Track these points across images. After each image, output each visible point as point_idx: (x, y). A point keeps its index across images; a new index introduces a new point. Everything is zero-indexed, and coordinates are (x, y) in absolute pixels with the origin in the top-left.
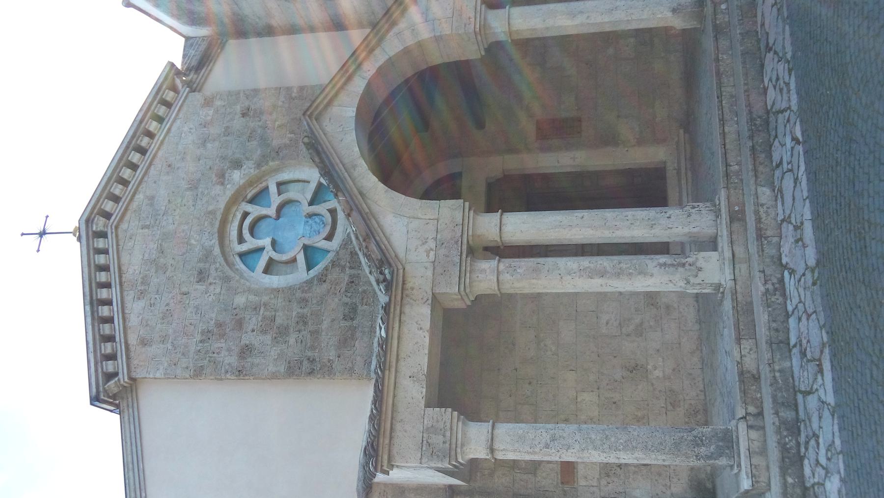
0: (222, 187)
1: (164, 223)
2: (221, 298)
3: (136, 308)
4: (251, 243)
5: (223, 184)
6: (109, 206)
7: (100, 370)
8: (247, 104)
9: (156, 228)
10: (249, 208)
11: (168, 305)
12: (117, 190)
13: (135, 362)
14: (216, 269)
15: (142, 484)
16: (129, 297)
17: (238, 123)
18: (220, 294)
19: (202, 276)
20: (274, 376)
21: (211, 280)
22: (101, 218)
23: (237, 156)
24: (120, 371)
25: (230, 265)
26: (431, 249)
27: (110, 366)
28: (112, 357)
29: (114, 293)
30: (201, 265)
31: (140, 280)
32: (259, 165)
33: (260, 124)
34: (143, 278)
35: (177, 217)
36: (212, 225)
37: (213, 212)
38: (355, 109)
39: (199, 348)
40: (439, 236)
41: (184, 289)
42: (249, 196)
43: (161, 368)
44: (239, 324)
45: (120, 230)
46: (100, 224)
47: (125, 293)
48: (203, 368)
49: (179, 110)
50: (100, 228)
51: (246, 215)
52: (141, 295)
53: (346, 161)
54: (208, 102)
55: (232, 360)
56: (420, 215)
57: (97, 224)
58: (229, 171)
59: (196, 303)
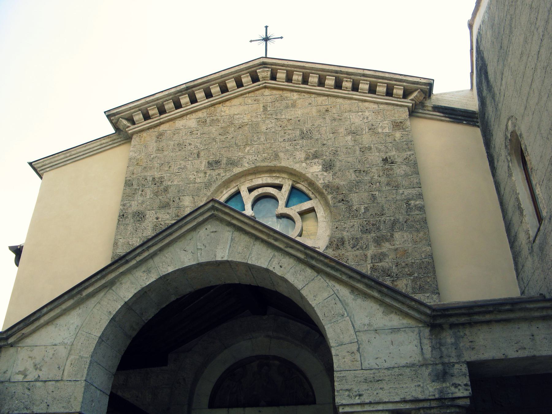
0: (303, 159)
1: (267, 122)
2: (191, 185)
3: (191, 122)
5: (307, 159)
6: (281, 75)
7: (132, 111)
8: (399, 160)
9: (263, 116)
10: (286, 189)
11: (190, 144)
12: (297, 77)
13: (144, 134)
14: (219, 174)
15: (56, 166)
16: (200, 114)
17: (375, 157)
18: (195, 183)
19: (214, 164)
20: (115, 244)
21: (209, 172)
22: (269, 73)
23: (338, 164)
24: (136, 126)
26: (26, 376)
27: (138, 117)
28: (147, 117)
29: (203, 101)
30: (224, 161)
31: (215, 118)
32: (327, 186)
33: (376, 177)
34: (217, 119)
35: (273, 130)
36: (264, 160)
37: (277, 156)
38: (225, 259)
39: (148, 178)
40: (39, 384)
41: (202, 154)
42: (299, 186)
43: (136, 155)
45: (264, 90)
46: (264, 73)
47: (205, 110)
48: (131, 186)
49: (387, 104)
50: (260, 76)
51: (279, 187)
52: (202, 122)
53: (157, 259)
54: (398, 125)
55: (134, 206)
56: (72, 357)
57: (263, 72)
58: (320, 161)
59: (189, 166)
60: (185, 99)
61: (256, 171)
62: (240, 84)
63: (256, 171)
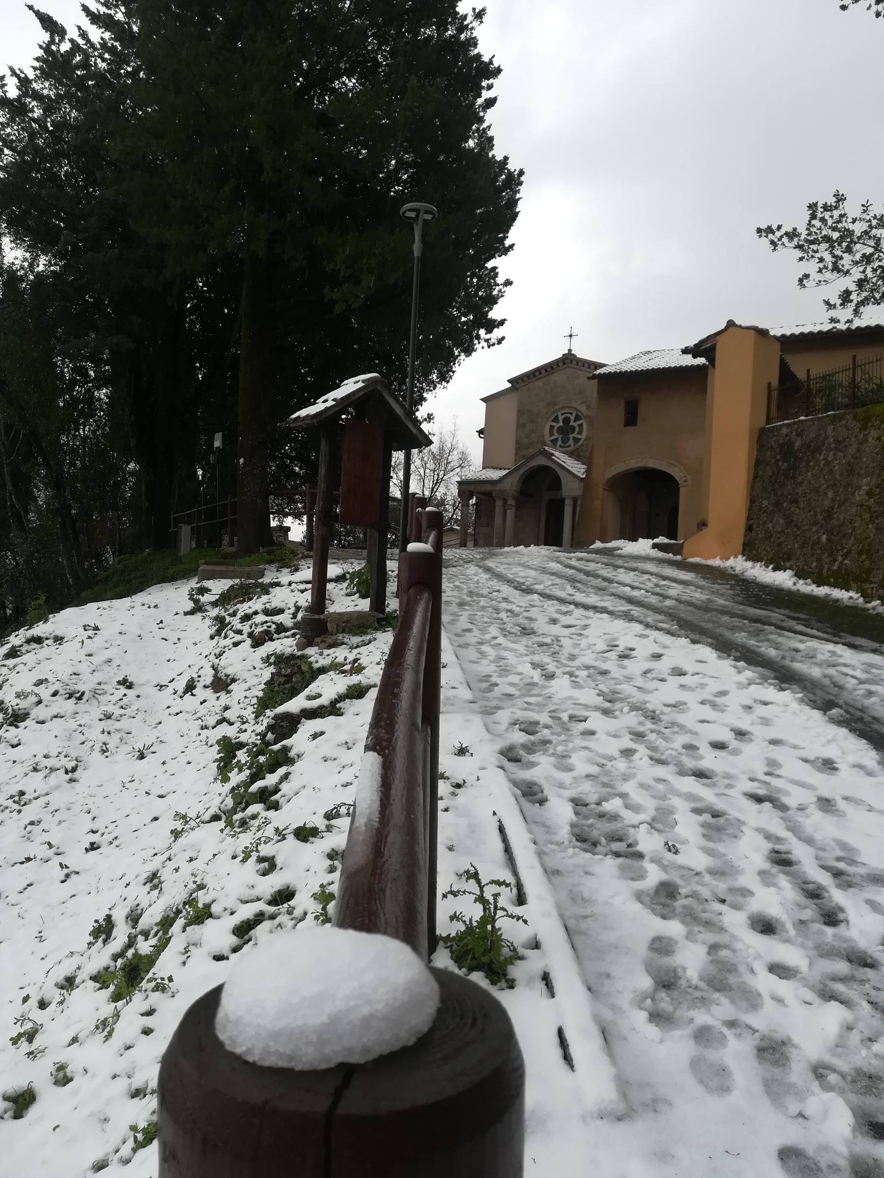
3: (539, 383)
4: (561, 418)
10: (574, 415)
16: (544, 380)
19: (549, 404)
25: (554, 413)
44: (532, 422)
46: (568, 361)
48: (520, 412)
51: (571, 414)
60: (537, 374)
61: (564, 408)
62: (558, 366)
63: (564, 408)
